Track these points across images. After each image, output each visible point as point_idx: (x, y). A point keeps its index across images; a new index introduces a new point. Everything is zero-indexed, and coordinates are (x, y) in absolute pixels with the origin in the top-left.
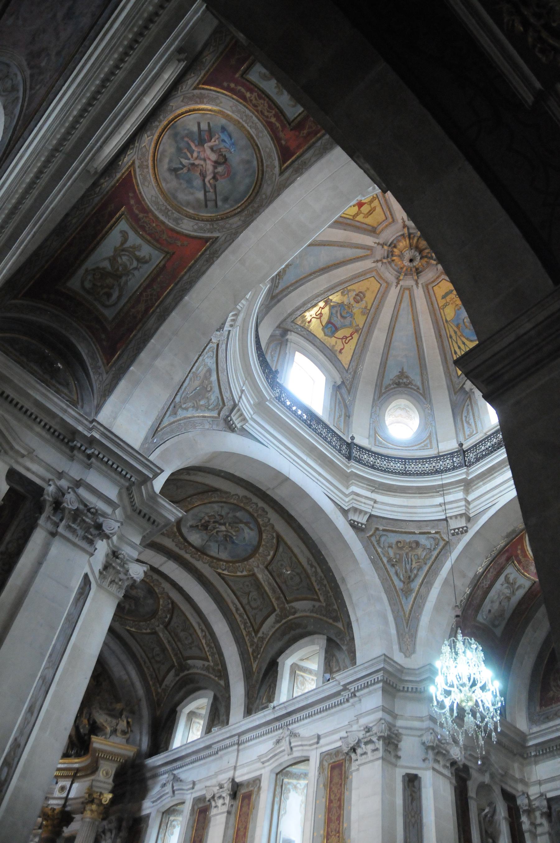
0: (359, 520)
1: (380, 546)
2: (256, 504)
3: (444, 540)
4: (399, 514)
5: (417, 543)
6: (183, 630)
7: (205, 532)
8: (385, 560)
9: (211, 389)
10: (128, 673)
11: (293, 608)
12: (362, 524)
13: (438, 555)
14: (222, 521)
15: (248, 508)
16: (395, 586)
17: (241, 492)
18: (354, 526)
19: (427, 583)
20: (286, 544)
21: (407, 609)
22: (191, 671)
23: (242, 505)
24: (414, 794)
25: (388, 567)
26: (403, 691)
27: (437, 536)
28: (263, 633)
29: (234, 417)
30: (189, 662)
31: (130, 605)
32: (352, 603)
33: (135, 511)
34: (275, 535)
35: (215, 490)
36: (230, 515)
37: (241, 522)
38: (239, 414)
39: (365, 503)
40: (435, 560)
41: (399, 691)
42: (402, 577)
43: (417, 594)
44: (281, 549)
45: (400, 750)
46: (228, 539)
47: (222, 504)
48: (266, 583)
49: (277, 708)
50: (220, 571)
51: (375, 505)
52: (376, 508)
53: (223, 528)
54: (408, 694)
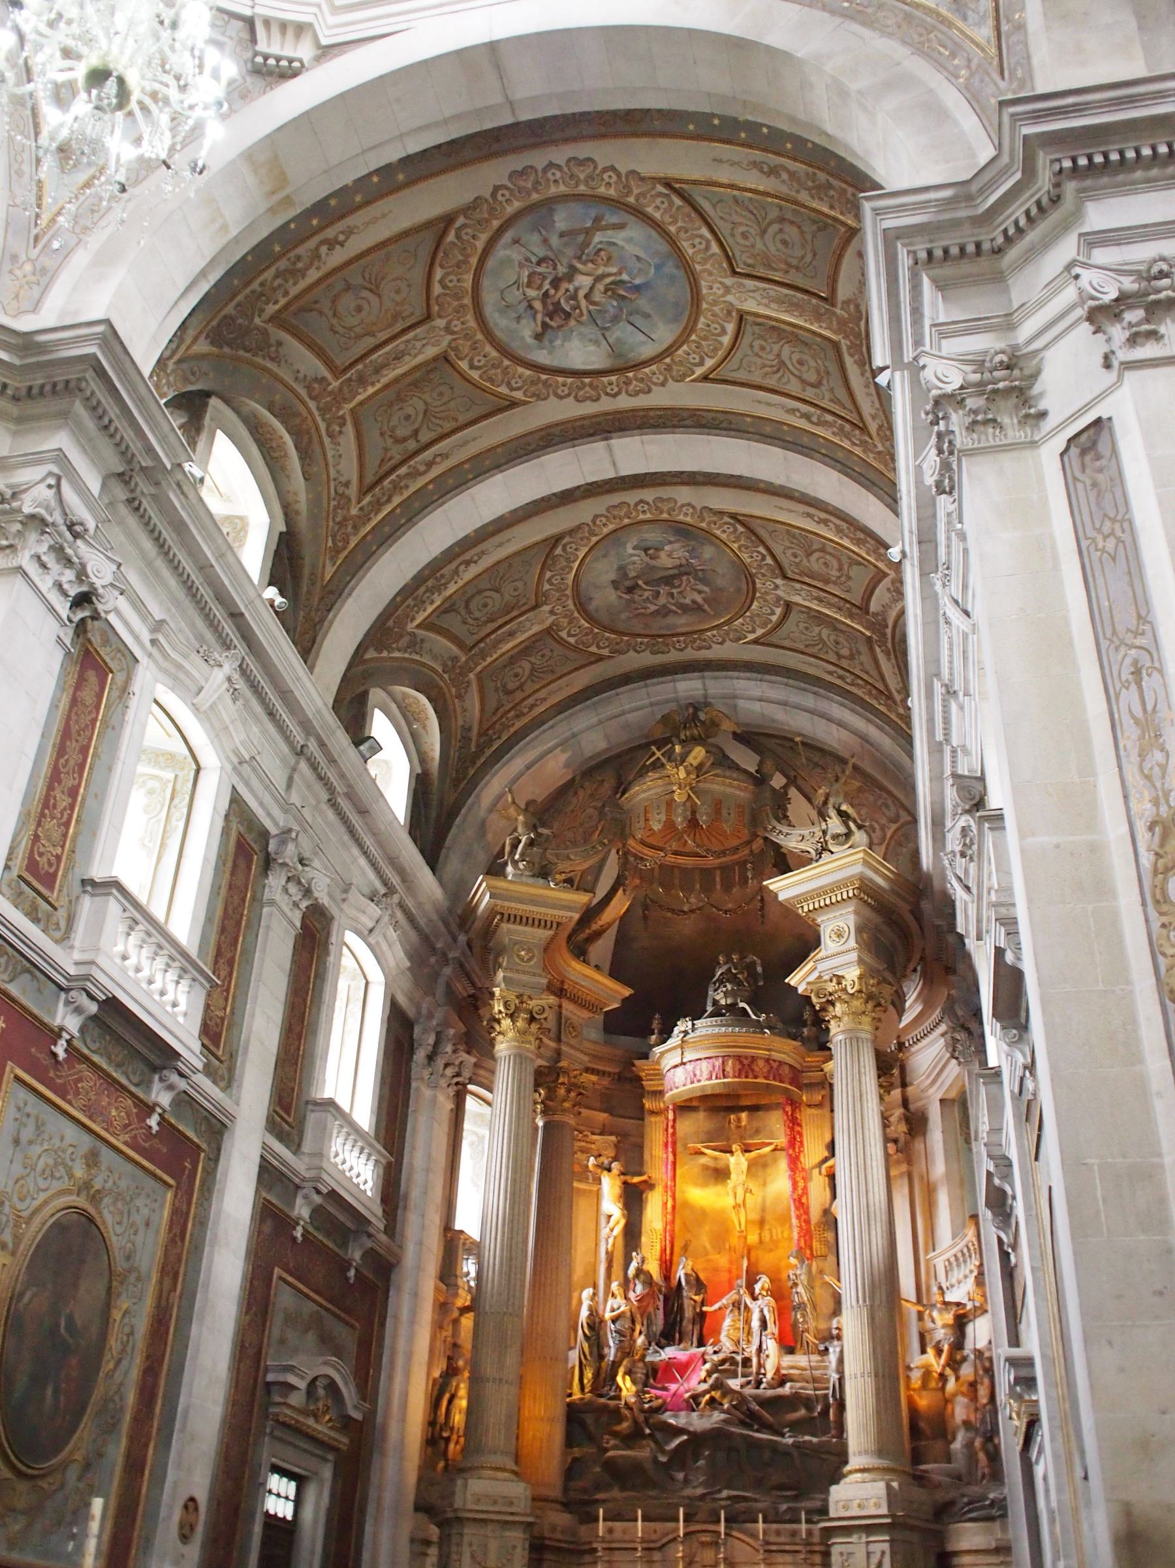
2: (551, 165)
6: (809, 555)
7: (572, 323)
10: (841, 724)
11: (847, 303)
14: (562, 270)
15: (553, 190)
20: (695, 182)
21: (984, 33)
22: (890, 623)
23: (535, 196)
24: (1100, 477)
26: (1009, 240)
28: (874, 418)
29: (271, 45)
30: (874, 606)
31: (700, 592)
32: (861, 159)
33: (16, 399)
34: (660, 188)
36: (555, 241)
37: (589, 232)
38: (275, 30)
41: (998, 251)
44: (706, 206)
45: (1041, 395)
46: (622, 292)
47: (508, 236)
48: (773, 305)
49: (907, 549)
50: (699, 371)
53: (584, 281)
54: (1032, 236)
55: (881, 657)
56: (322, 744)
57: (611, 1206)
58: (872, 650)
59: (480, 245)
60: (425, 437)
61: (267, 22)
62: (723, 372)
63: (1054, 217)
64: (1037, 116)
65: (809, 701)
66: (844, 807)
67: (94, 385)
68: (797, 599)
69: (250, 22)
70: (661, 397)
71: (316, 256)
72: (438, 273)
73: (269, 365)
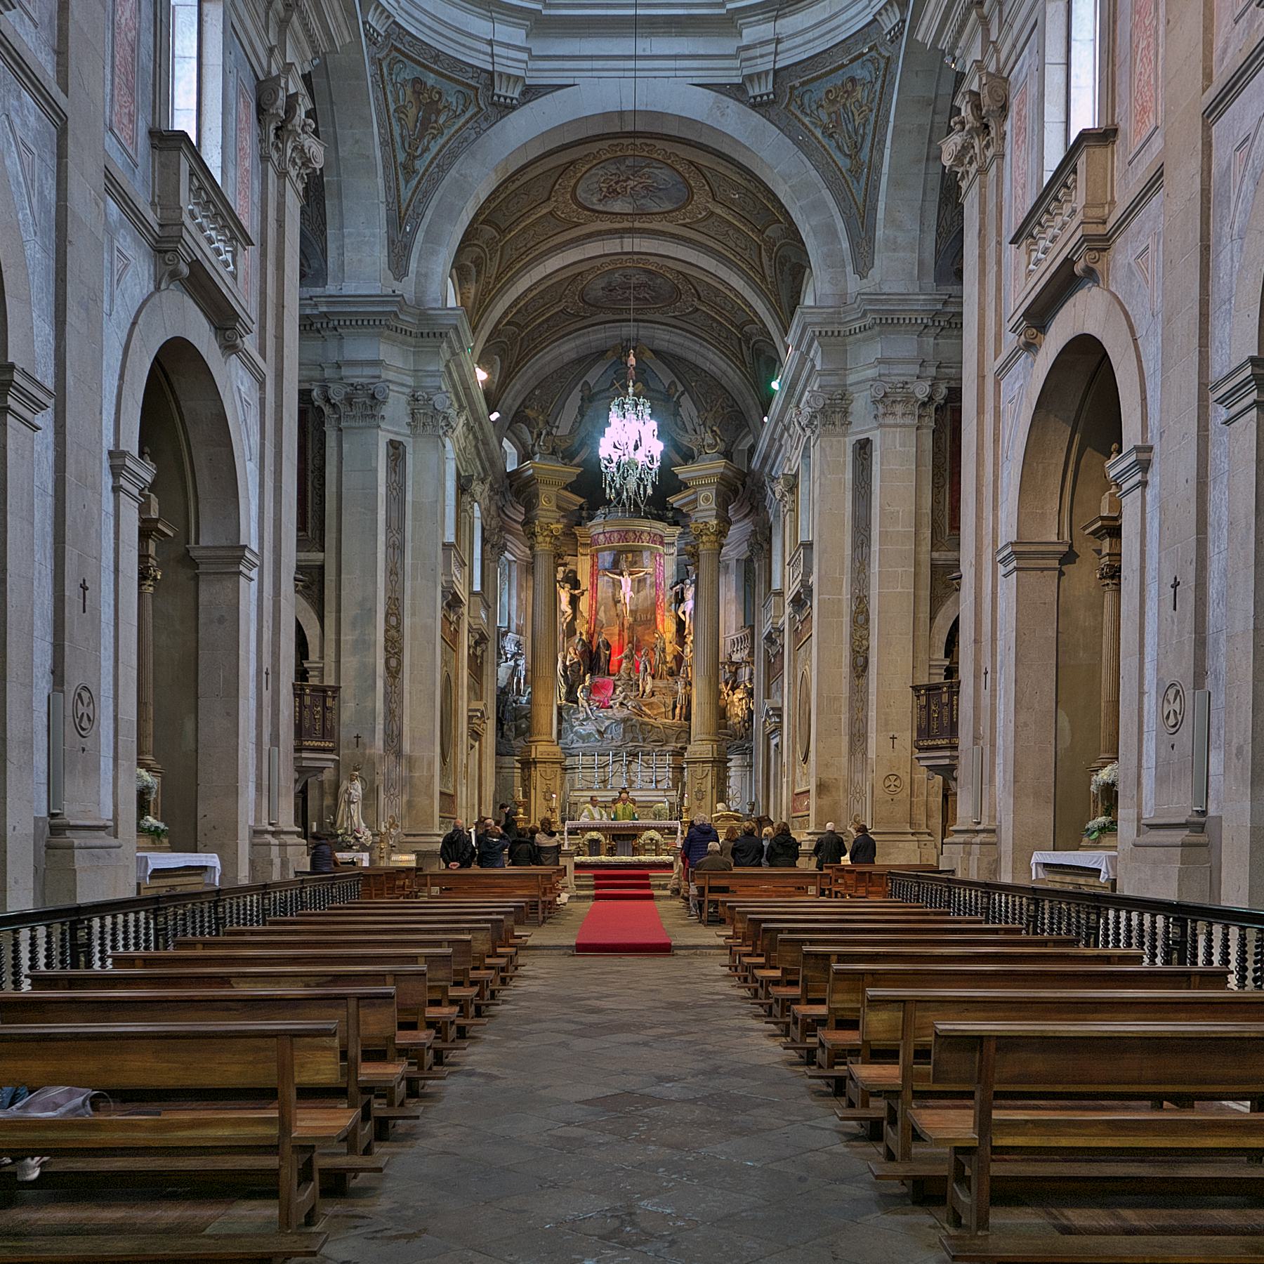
0: (764, 91)
1: (807, 114)
3: (884, 57)
4: (817, 42)
5: (852, 80)
8: (818, 133)
9: (440, 93)
10: (712, 363)
12: (768, 95)
13: (882, 87)
16: (839, 169)
17: (605, 144)
18: (758, 105)
19: (878, 143)
21: (860, 201)
23: (619, 153)
25: (824, 141)
27: (873, 53)
29: (501, 90)
30: (745, 329)
35: (572, 163)
39: (762, 56)
40: (880, 99)
42: (846, 149)
43: (869, 168)
51: (780, 47)
52: (782, 52)
53: (631, 183)
55: (744, 347)
56: (480, 424)
57: (565, 605)
58: (740, 343)
59: (584, 170)
60: (528, 246)
61: (501, 74)
62: (695, 226)
63: (869, 332)
64: (871, 301)
65: (697, 348)
66: (715, 428)
67: (452, 334)
68: (704, 309)
69: (491, 74)
70: (655, 226)
71: (507, 187)
72: (560, 181)
73: (476, 242)
